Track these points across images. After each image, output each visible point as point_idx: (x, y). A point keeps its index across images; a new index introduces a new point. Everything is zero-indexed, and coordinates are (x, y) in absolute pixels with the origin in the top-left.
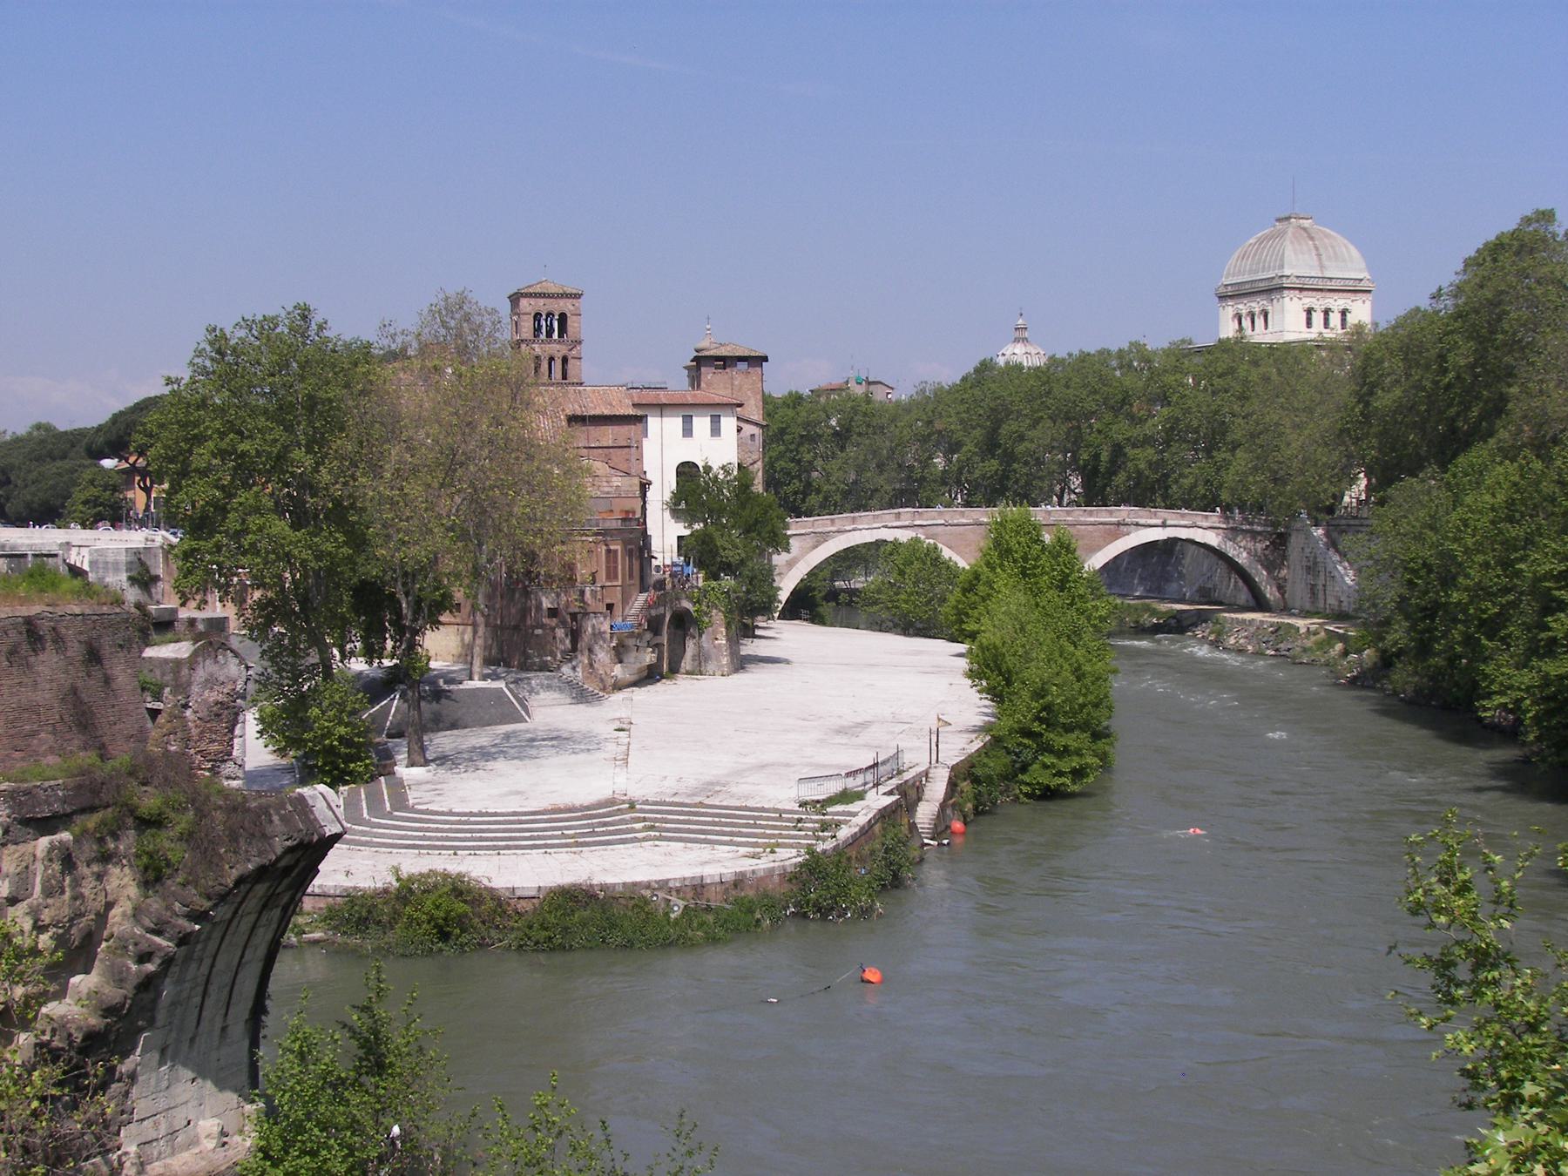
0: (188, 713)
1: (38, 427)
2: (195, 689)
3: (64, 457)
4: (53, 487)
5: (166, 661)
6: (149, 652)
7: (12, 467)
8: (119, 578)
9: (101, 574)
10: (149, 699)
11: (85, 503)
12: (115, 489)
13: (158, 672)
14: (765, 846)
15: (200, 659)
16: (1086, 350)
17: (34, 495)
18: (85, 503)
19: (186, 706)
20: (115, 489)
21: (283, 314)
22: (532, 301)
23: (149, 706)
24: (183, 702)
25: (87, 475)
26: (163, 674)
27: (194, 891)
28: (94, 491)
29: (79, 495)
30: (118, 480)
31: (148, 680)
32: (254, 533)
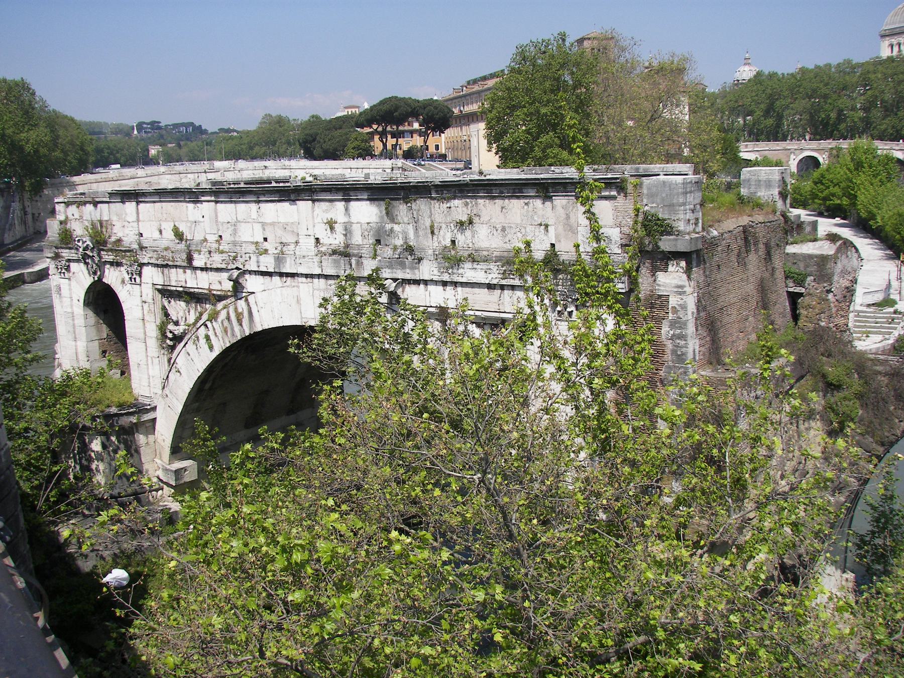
0: (830, 296)
1: (313, 117)
2: (836, 278)
3: (340, 128)
4: (338, 142)
5: (810, 257)
6: (790, 249)
7: (317, 134)
8: (771, 193)
9: (752, 190)
10: (791, 284)
11: (353, 148)
12: (366, 141)
13: (802, 265)
14: (863, 333)
15: (839, 255)
16: (818, 64)
17: (330, 146)
18: (353, 148)
19: (829, 291)
20: (366, 141)
21: (552, 39)
22: (590, 42)
23: (790, 290)
24: (828, 288)
25: (354, 135)
26: (806, 266)
27: (871, 439)
28: (357, 143)
29: (350, 145)
30: (367, 137)
31: (792, 270)
32: (552, 158)
